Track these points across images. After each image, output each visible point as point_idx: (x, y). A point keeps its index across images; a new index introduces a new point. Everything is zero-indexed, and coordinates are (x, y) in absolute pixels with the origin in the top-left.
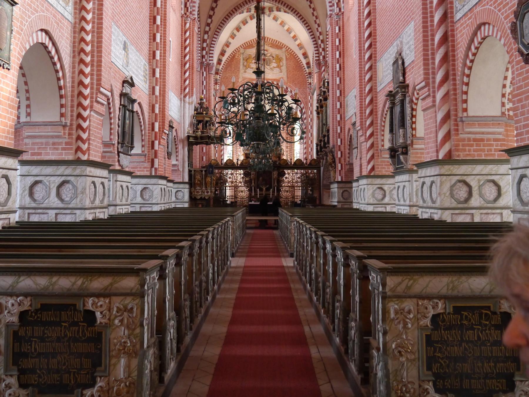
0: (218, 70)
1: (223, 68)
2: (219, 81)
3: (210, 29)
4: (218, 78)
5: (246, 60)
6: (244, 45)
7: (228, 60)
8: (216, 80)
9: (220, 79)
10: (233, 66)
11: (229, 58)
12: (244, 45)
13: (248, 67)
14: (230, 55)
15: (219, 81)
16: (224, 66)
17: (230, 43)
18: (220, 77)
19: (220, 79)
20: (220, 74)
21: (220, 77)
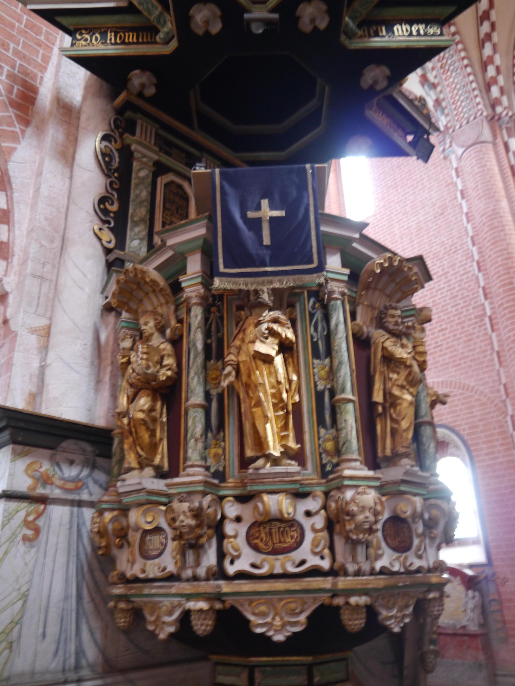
3: (493, 26)
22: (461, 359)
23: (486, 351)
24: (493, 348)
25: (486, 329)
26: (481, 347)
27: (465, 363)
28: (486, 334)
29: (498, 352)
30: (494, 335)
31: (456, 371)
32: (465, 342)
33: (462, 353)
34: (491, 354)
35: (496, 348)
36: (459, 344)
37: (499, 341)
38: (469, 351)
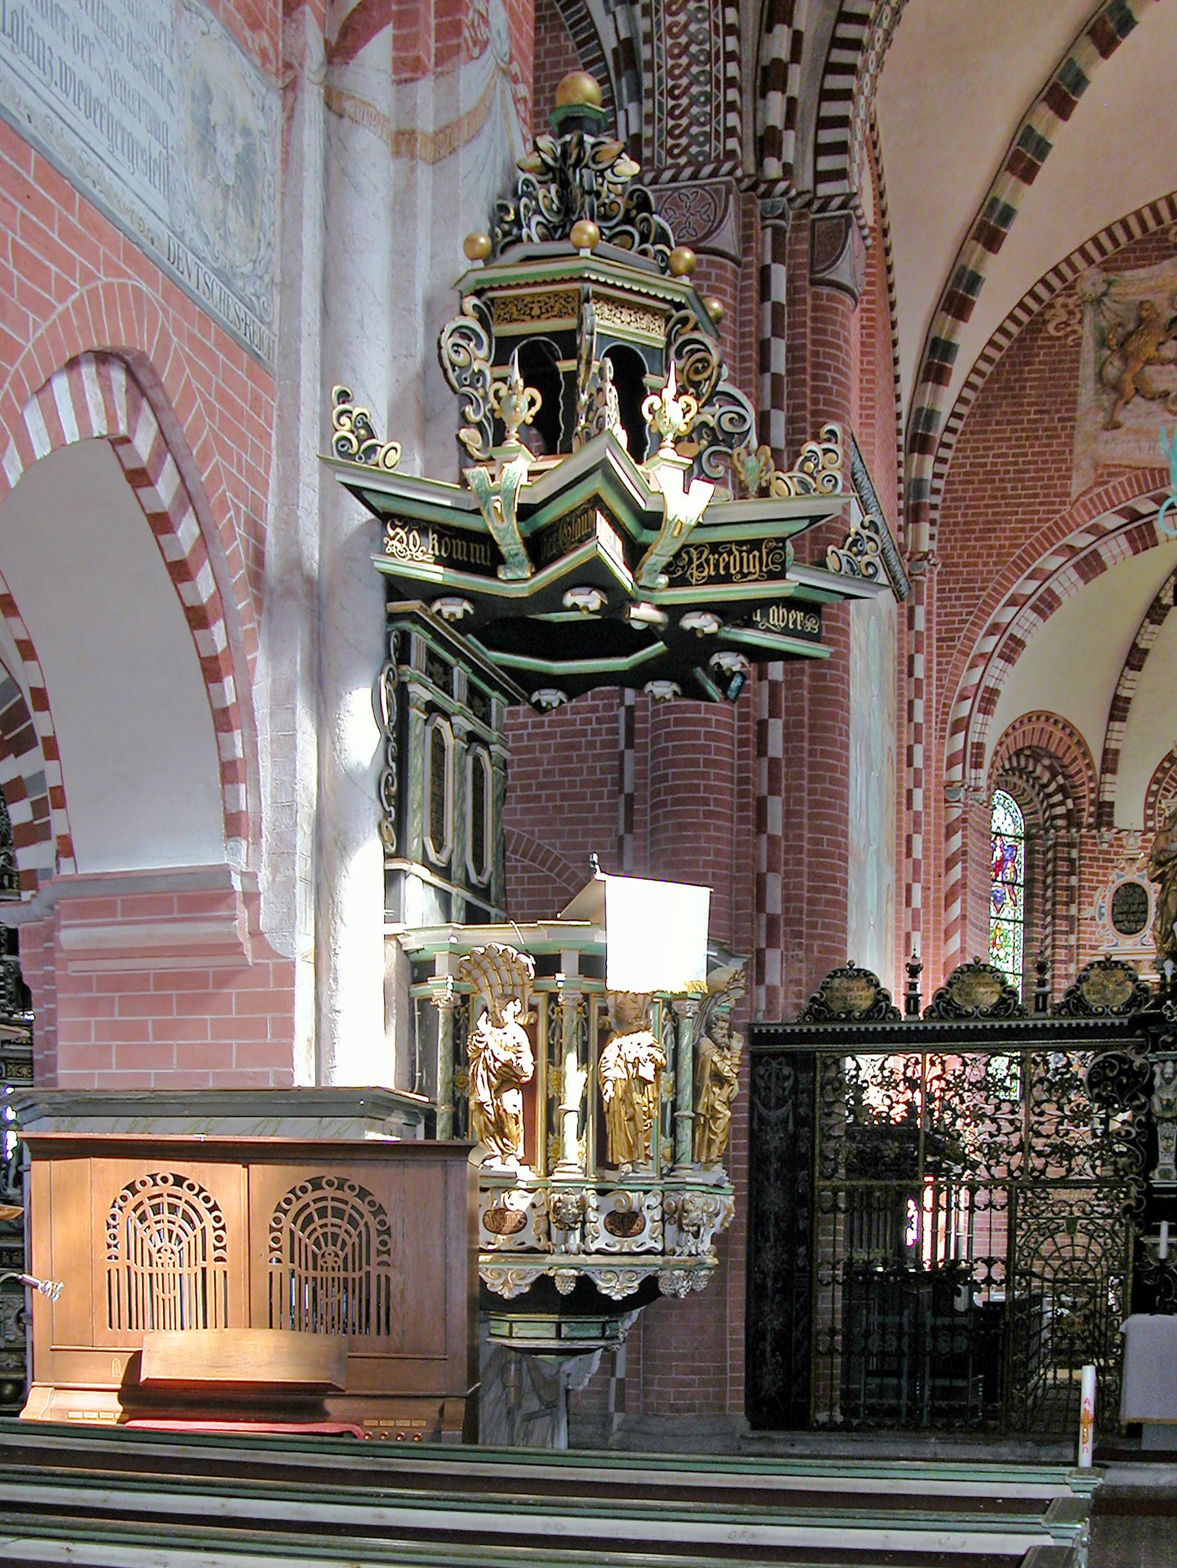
0: (930, 416)
1: (963, 410)
2: (937, 500)
4: (928, 475)
5: (1122, 345)
6: (1104, 240)
7: (996, 355)
8: (917, 487)
9: (940, 484)
10: (1031, 395)
11: (1001, 340)
12: (1104, 240)
13: (1129, 388)
14: (1011, 317)
15: (937, 500)
16: (969, 394)
17: (1007, 215)
18: (944, 469)
19: (940, 484)
20: (943, 453)
21: (944, 469)
22: (541, 786)
23: (602, 783)
24: (620, 782)
25: (615, 731)
26: (592, 770)
27: (550, 798)
28: (615, 743)
29: (630, 799)
30: (629, 754)
31: (525, 811)
32: (559, 747)
33: (548, 773)
34: (611, 795)
35: (628, 788)
36: (544, 749)
37: (639, 775)
38: (563, 773)
